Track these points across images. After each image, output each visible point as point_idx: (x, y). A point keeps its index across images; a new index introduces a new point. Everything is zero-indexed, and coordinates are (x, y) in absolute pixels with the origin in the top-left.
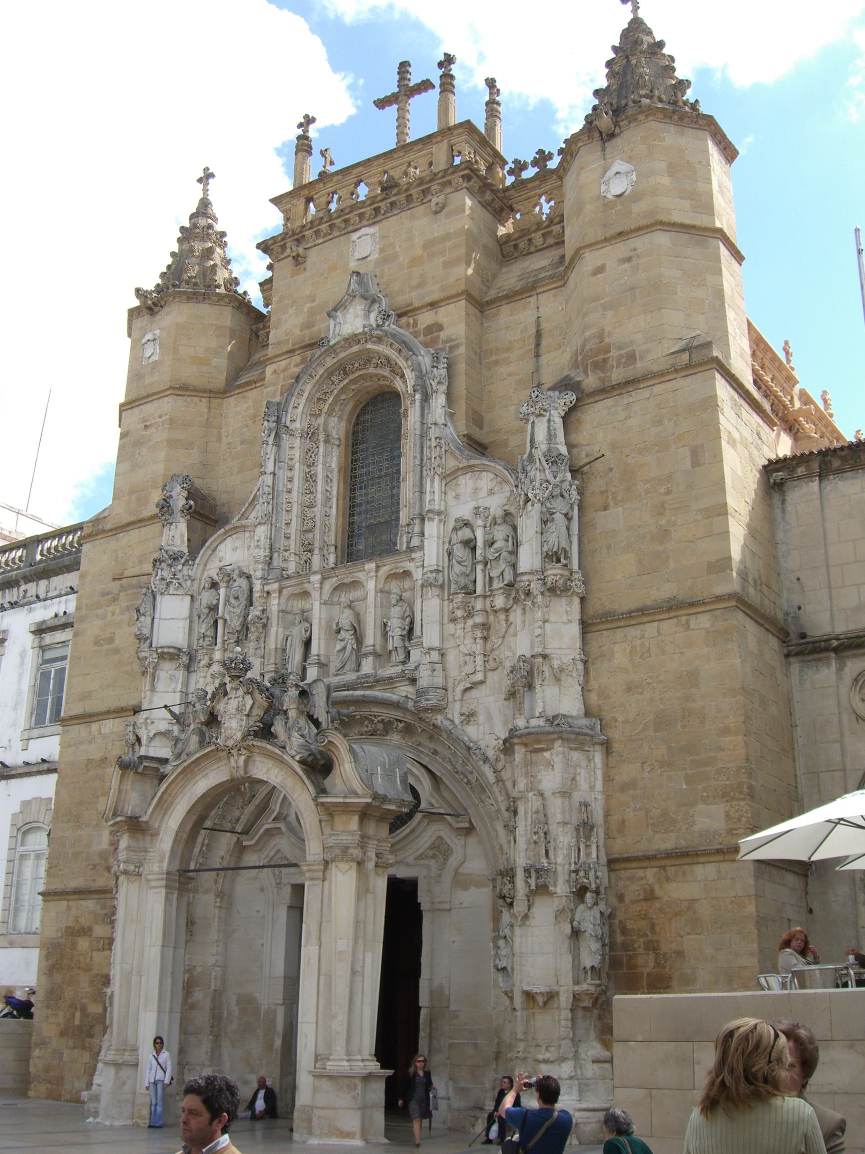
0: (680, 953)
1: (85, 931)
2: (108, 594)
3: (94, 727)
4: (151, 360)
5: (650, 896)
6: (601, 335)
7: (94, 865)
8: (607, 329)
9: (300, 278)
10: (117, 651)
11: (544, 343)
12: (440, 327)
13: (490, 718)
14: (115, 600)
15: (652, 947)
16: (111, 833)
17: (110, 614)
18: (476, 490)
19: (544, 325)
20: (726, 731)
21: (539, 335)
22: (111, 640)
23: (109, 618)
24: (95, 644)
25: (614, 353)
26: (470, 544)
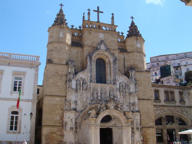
0: (148, 138)
1: (55, 133)
2: (55, 75)
3: (54, 98)
4: (61, 37)
5: (145, 132)
6: (137, 64)
7: (56, 122)
8: (138, 64)
9: (90, 35)
10: (58, 86)
11: (125, 61)
12: (114, 54)
13: (126, 109)
14: (56, 77)
15: (146, 138)
16: (59, 117)
17: (55, 79)
18: (122, 79)
19: (125, 59)
20: (152, 115)
21: (124, 60)
22: (56, 84)
23: (55, 79)
24: (53, 83)
25: (139, 67)
26: (123, 86)
